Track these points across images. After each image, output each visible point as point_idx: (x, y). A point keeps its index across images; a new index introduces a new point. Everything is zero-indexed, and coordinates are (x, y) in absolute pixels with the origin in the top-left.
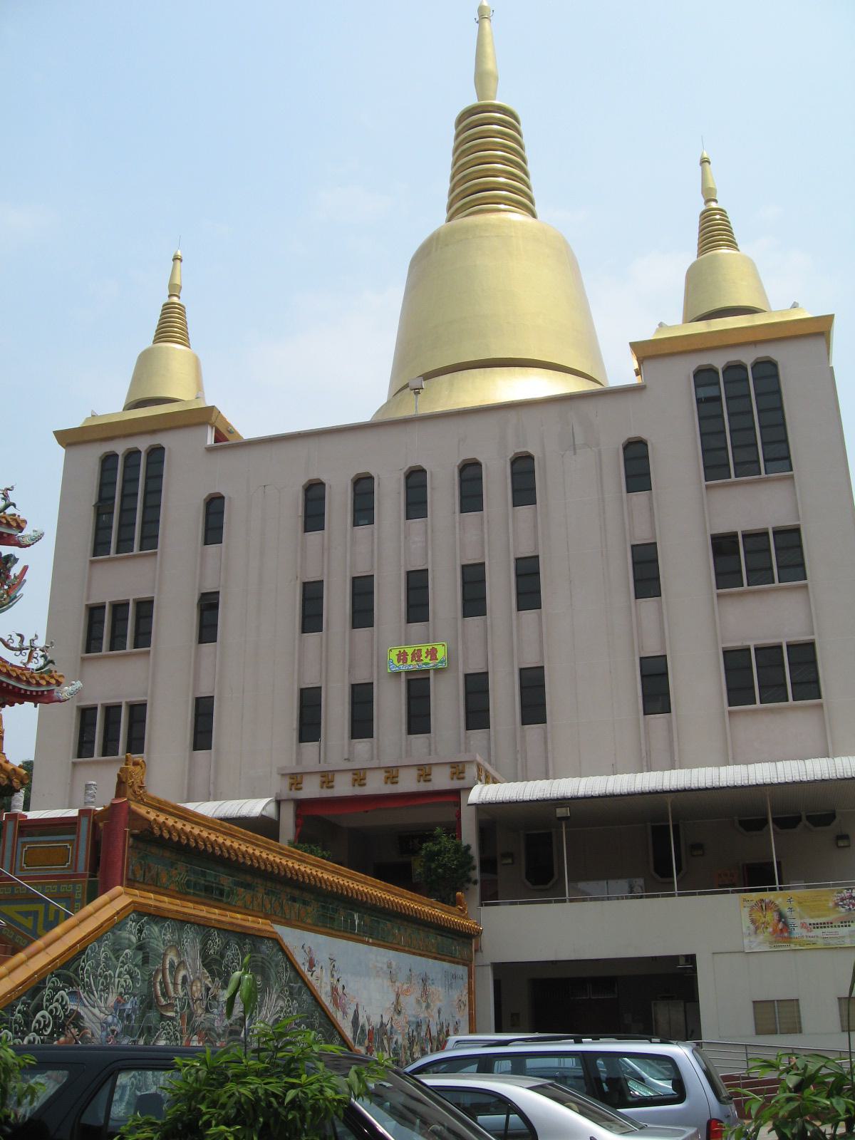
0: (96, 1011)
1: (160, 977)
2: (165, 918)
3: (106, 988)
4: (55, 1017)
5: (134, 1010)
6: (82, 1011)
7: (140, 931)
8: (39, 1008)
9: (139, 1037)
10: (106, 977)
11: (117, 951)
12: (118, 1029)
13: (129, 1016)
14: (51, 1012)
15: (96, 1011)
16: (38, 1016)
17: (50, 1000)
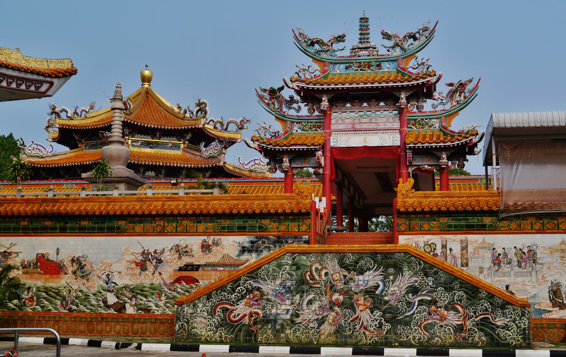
0: (269, 286)
1: (309, 273)
2: (311, 253)
3: (274, 279)
4: (247, 289)
5: (292, 285)
6: (261, 286)
7: (294, 259)
8: (239, 286)
9: (297, 294)
10: (274, 275)
11: (280, 266)
12: (283, 291)
13: (288, 287)
14: (245, 287)
15: (269, 286)
16: (238, 288)
17: (244, 284)
